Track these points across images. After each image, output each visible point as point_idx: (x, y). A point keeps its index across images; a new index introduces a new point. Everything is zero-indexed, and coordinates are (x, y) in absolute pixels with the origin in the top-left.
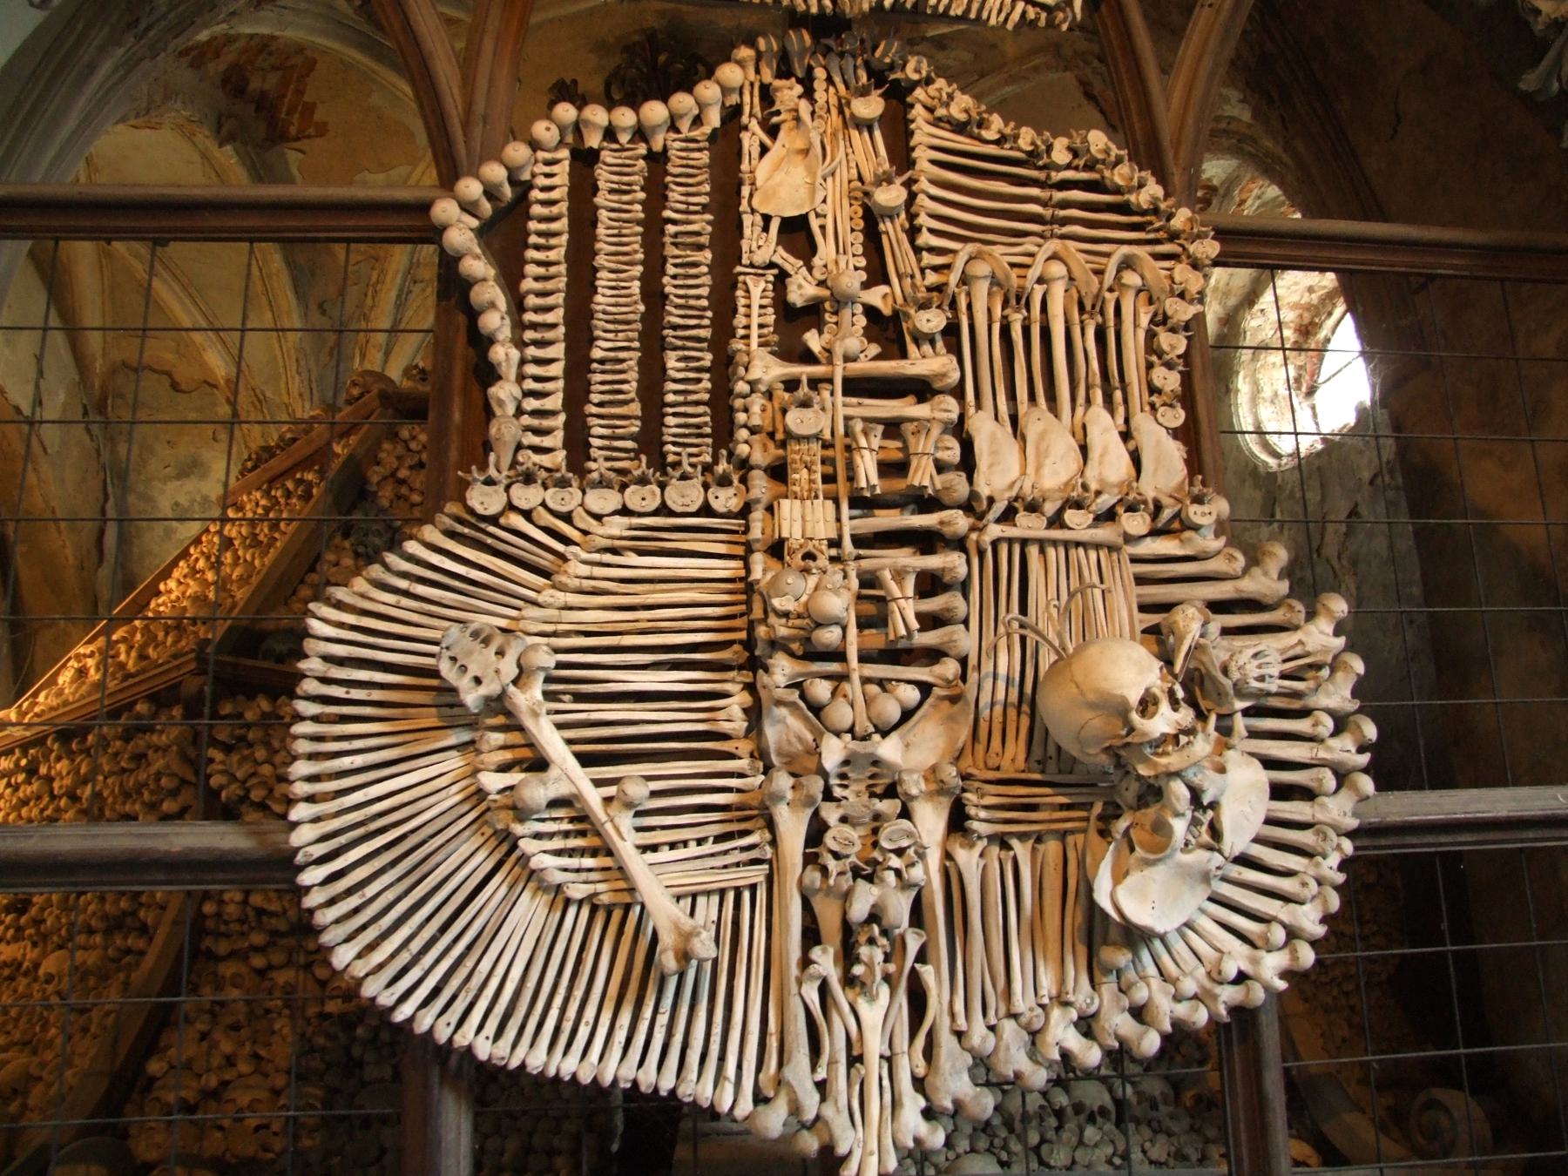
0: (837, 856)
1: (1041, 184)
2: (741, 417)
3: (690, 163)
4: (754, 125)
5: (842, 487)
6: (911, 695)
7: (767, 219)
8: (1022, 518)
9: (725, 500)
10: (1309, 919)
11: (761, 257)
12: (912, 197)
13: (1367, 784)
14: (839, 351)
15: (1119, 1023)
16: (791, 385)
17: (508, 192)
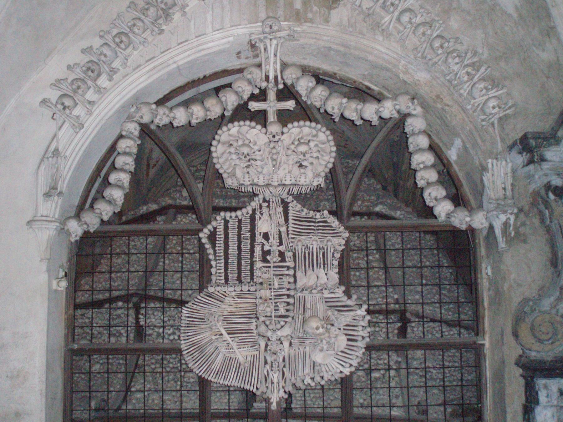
0: (270, 350)
1: (314, 222)
2: (255, 274)
3: (246, 221)
4: (258, 213)
5: (272, 287)
6: (282, 323)
7: (260, 233)
8: (304, 292)
9: (252, 289)
10: (355, 363)
11: (259, 241)
12: (288, 228)
13: (368, 339)
14: (272, 261)
15: (318, 379)
16: (264, 267)
17: (212, 230)
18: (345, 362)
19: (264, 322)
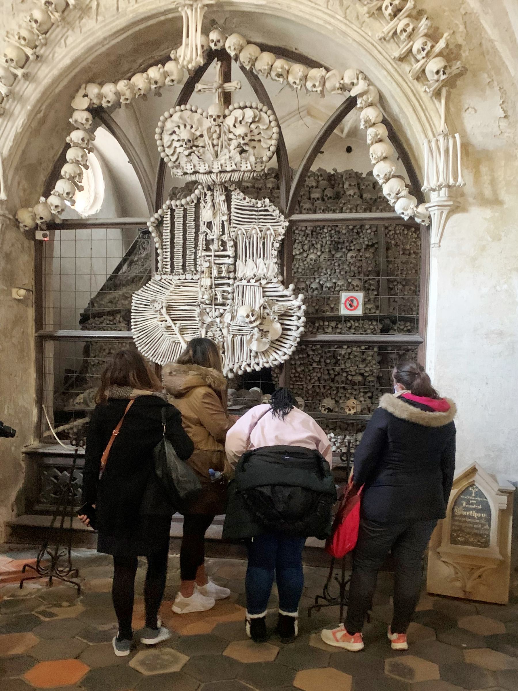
3: (191, 210)
4: (203, 202)
9: (196, 277)
10: (289, 352)
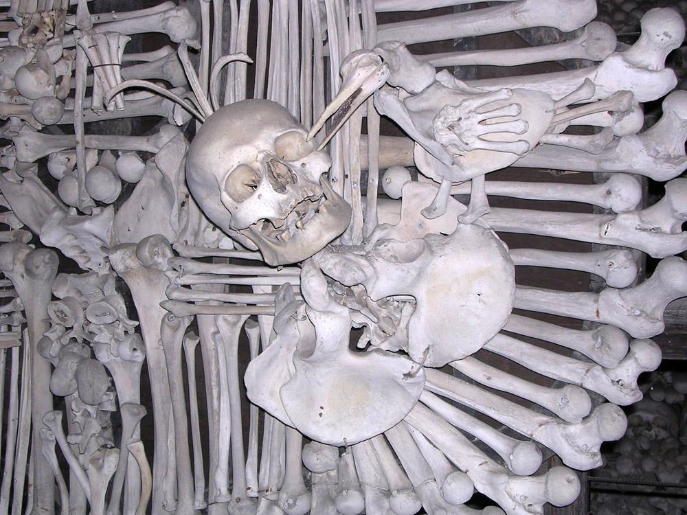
10: (581, 445)
18: (509, 432)
19: (43, 163)
